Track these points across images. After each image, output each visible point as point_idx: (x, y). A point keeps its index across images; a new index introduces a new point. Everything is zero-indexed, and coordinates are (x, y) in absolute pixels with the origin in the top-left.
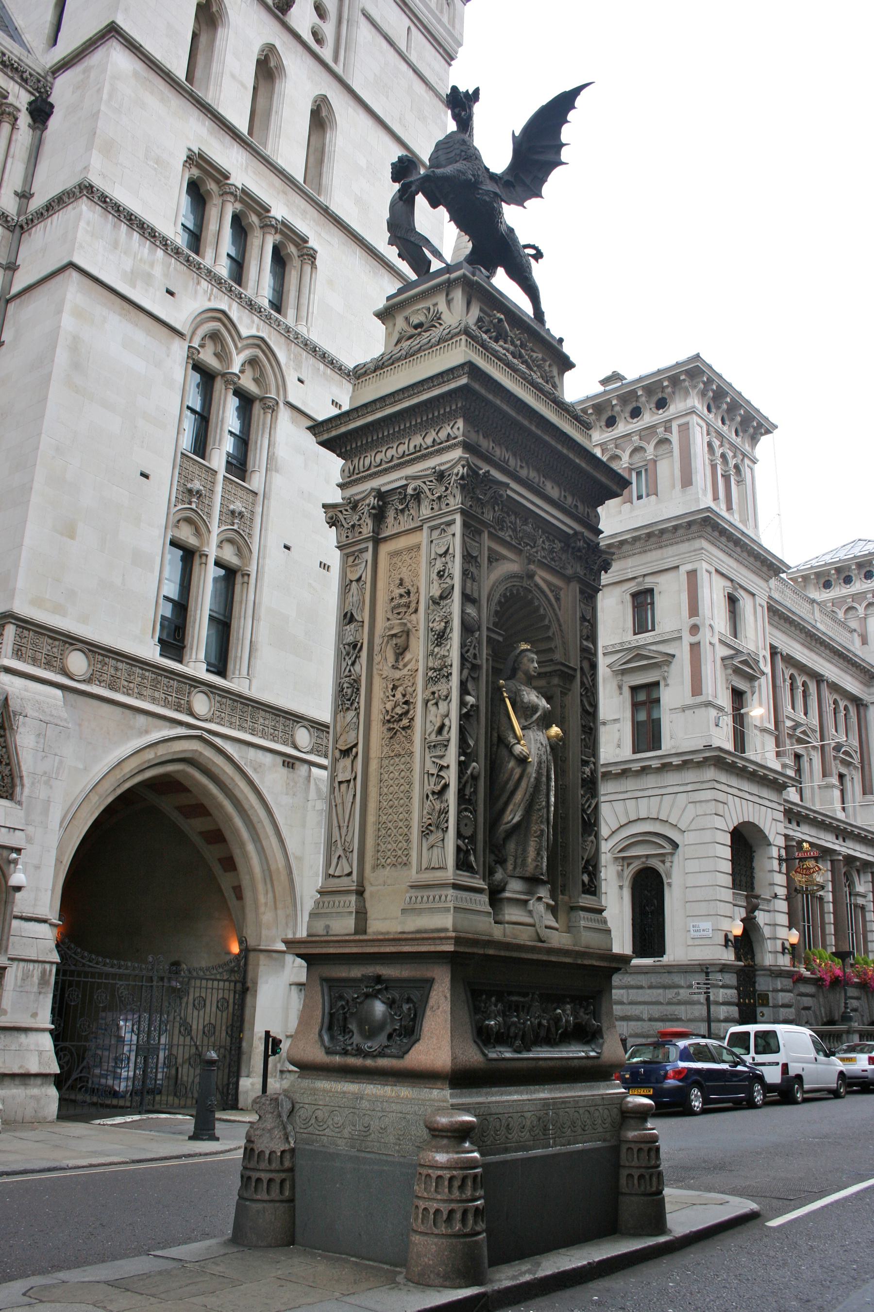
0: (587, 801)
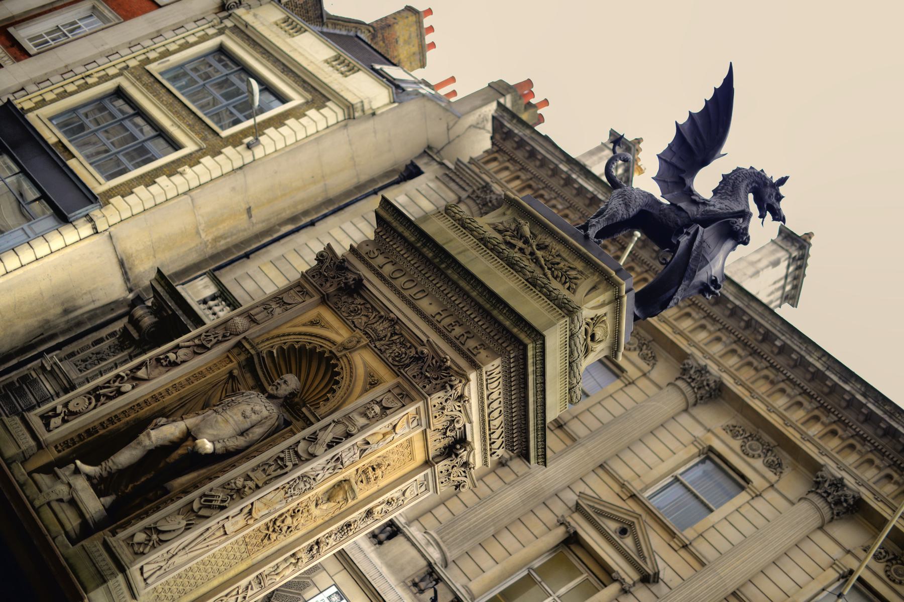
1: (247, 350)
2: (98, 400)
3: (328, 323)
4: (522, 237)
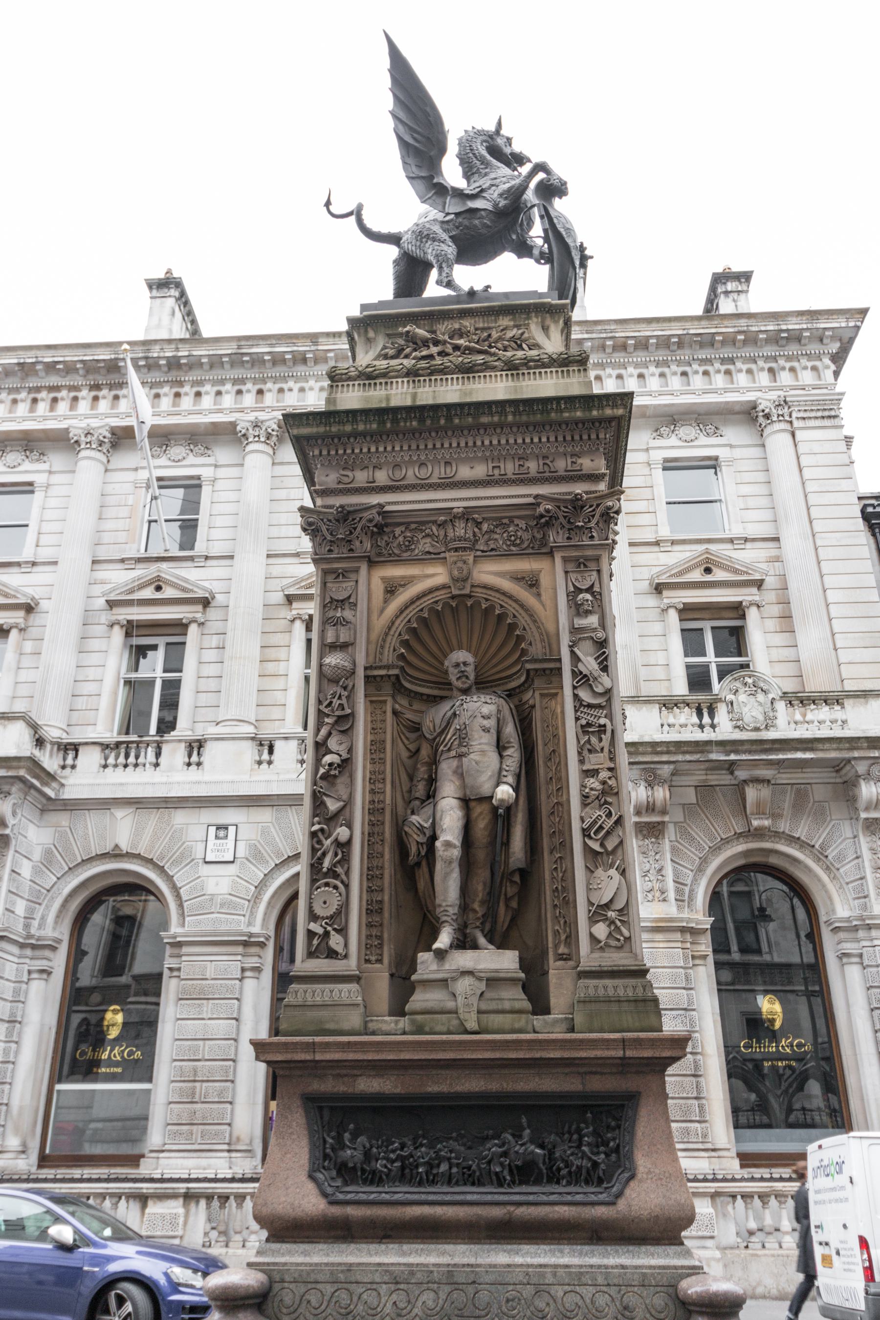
0: (595, 822)
1: (382, 676)
2: (336, 876)
3: (403, 577)
4: (425, 343)
